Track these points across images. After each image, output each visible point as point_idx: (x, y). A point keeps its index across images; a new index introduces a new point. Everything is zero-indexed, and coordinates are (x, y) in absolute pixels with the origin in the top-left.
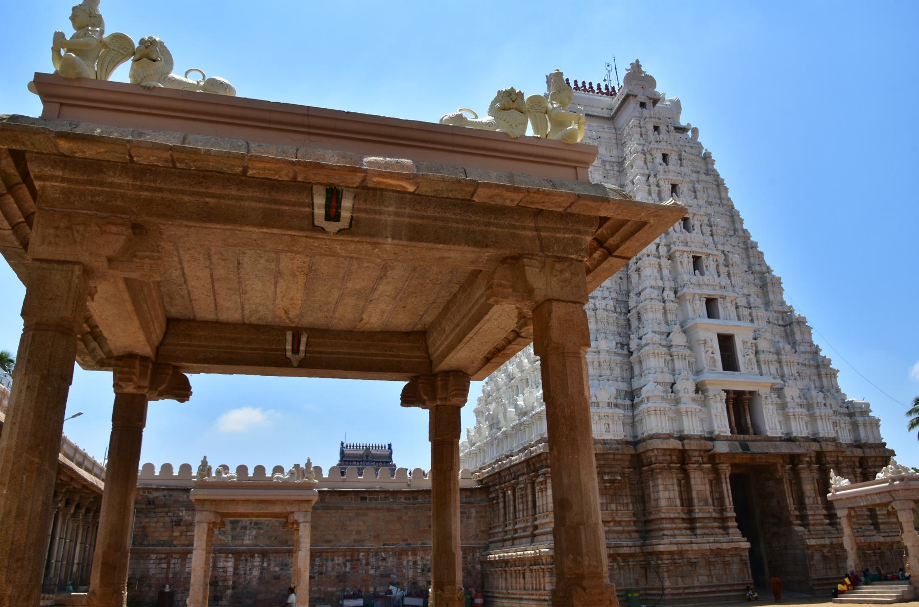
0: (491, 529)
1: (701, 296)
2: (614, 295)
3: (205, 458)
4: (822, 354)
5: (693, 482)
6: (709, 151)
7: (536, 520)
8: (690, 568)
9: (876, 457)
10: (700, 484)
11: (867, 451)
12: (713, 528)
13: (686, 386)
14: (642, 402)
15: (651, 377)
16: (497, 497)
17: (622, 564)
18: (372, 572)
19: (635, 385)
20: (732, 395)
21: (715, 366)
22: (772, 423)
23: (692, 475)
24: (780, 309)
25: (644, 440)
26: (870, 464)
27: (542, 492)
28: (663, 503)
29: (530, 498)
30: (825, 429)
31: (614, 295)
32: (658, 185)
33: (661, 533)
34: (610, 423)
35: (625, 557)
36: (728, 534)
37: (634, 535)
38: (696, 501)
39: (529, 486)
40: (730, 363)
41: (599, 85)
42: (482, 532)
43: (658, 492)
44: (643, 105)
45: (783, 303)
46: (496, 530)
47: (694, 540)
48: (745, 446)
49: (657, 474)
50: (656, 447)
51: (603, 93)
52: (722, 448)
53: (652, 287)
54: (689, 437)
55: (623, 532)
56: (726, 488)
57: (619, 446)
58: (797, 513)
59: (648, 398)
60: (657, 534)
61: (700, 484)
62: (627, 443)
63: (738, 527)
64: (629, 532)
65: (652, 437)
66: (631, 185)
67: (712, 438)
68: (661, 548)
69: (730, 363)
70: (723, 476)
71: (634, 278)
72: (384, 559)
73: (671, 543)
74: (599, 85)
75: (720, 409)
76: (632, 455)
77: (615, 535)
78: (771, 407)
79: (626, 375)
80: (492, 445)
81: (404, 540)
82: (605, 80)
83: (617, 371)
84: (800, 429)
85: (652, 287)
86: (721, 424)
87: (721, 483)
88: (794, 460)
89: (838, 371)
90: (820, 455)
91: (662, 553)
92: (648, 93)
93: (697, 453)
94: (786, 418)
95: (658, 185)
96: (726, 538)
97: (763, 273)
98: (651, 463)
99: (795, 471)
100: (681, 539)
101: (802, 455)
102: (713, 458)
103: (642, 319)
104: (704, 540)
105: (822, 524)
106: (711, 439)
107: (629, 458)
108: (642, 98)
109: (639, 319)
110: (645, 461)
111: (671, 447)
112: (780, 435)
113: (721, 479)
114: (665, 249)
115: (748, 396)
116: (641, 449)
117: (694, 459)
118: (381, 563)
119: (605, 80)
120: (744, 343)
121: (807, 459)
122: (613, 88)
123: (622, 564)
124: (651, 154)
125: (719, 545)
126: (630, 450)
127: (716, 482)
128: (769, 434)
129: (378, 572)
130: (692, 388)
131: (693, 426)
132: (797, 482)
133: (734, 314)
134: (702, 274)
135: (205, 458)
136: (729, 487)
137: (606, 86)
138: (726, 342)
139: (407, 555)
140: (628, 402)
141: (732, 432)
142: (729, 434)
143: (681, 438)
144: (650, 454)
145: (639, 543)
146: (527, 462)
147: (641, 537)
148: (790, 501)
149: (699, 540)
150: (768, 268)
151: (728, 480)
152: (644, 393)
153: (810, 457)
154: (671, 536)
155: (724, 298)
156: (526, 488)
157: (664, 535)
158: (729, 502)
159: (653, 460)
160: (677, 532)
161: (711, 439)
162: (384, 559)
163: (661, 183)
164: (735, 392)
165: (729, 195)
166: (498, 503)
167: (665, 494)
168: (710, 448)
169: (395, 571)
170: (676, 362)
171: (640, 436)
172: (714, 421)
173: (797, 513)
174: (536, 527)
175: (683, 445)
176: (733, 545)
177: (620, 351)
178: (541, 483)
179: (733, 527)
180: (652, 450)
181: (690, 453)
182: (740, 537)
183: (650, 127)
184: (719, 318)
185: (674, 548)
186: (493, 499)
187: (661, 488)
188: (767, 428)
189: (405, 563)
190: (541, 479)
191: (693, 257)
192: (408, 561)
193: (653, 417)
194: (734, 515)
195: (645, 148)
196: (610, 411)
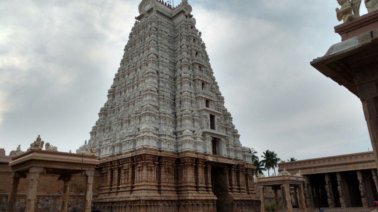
0: (100, 187)
1: (205, 98)
2: (170, 92)
3: (39, 136)
4: (235, 128)
5: (199, 172)
7: (119, 185)
8: (197, 207)
9: (250, 169)
10: (201, 172)
11: (248, 166)
12: (204, 191)
13: (199, 133)
14: (183, 137)
15: (188, 127)
16: (107, 173)
17: (170, 204)
18: (40, 207)
19: (179, 129)
21: (208, 127)
22: (224, 152)
23: (199, 169)
25: (182, 153)
26: (249, 171)
27: (139, 171)
28: (189, 180)
29: (130, 174)
30: (240, 156)
31: (170, 92)
33: (187, 192)
34: (170, 144)
35: (172, 201)
36: (209, 194)
37: (175, 192)
38: (199, 179)
39: (130, 169)
40: (213, 127)
41: (166, 3)
42: (96, 188)
43: (187, 174)
44: (186, 16)
45: (224, 107)
46: (105, 188)
47: (198, 195)
48: (217, 160)
49: (188, 167)
50: (189, 156)
51: (166, 6)
52: (210, 159)
53: (187, 91)
54: (199, 153)
55: (170, 190)
56: (209, 175)
57: (173, 154)
58: (230, 187)
59: (186, 136)
60: (184, 192)
61: (201, 172)
62: (174, 153)
63: (212, 191)
64: (173, 191)
65: (187, 152)
66: (180, 48)
67: (205, 154)
68: (189, 198)
69: (213, 127)
70: (209, 170)
71: (179, 87)
72: (47, 201)
73: (192, 196)
74: (166, 3)
76: (177, 159)
77: (168, 192)
78: (225, 145)
79: (174, 125)
80: (107, 149)
81: (58, 191)
82: (168, 2)
83: (171, 123)
84: (232, 155)
85: (187, 91)
86: (210, 150)
87: (208, 173)
88: (230, 166)
89: (240, 136)
90: (238, 165)
91: (189, 200)
92: (189, 13)
93: (202, 160)
94: (228, 150)
95: (191, 51)
96: (209, 195)
97: (218, 94)
98: (185, 162)
99: (230, 171)
100: (194, 195)
101: (233, 165)
102: (207, 163)
103: (183, 104)
104: (203, 195)
105: (237, 192)
106: (206, 155)
107: (175, 160)
108: (187, 13)
109: (180, 103)
110: (182, 161)
112: (227, 156)
113: (208, 171)
114: (193, 77)
116: (181, 156)
117: (200, 162)
118: (45, 202)
119: (168, 2)
120: (218, 119)
121: (234, 167)
122: (171, 6)
123: (170, 204)
124: (189, 38)
125: (207, 198)
126: (176, 156)
127: (206, 173)
128: (223, 156)
129: (43, 207)
130: (201, 134)
131: (200, 149)
132: (230, 176)
133: (214, 108)
135: (39, 136)
136: (210, 175)
137: (168, 4)
138: (212, 117)
139: (59, 199)
140: (175, 136)
142: (211, 154)
143: (197, 153)
144: (186, 159)
145: (177, 195)
146: (132, 158)
147: (177, 194)
148: (228, 182)
149: (200, 195)
150: (220, 93)
151: (210, 172)
152: (185, 133)
153: (235, 166)
154: (191, 193)
155: (211, 100)
156: (128, 169)
157: (189, 193)
158: (210, 181)
159: (186, 161)
160: (193, 192)
161: (206, 155)
162: (47, 201)
163: (193, 50)
164: (214, 138)
165: (210, 62)
166: (107, 176)
167: (189, 176)
168: (206, 159)
169: (52, 206)
170: (195, 123)
171: (179, 151)
172: (207, 148)
173: (230, 187)
174: (133, 187)
175: (198, 156)
176: (212, 198)
177: (172, 115)
178: (140, 167)
179: (210, 191)
180: (187, 157)
181: (200, 160)
182: (213, 195)
183: (190, 26)
184: (209, 108)
185: (193, 198)
186: (104, 173)
187: (188, 173)
189: (58, 203)
190: (139, 165)
191: (202, 83)
192: (59, 202)
194: (211, 186)
195: (187, 35)
196: (169, 139)
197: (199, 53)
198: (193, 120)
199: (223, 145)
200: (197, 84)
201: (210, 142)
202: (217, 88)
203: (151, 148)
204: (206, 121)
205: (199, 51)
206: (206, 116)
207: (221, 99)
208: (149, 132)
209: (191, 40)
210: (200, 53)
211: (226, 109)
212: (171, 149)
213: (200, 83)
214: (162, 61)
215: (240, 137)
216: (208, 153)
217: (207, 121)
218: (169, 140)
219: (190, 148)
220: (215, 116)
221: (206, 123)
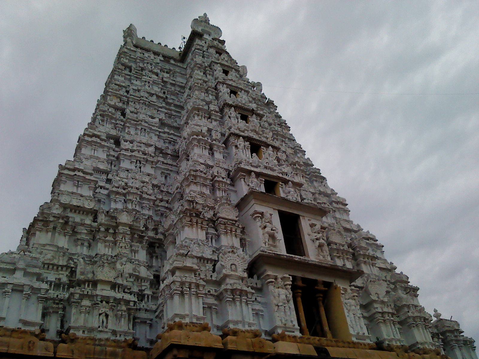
6: (271, 99)
20: (300, 283)
24: (348, 226)
32: (216, 88)
57: (119, 350)
75: (283, 297)
94: (371, 320)
111: (203, 344)
115: (321, 287)
120: (312, 226)
128: (354, 339)
134: (260, 157)
141: (301, 331)
142: (298, 334)
164: (304, 280)
188: (352, 331)
193: (176, 298)
197: (239, 93)
198: (216, 231)
199: (347, 301)
200: (234, 147)
201: (283, 292)
202: (322, 182)
203: (7, 330)
204: (265, 227)
205: (237, 87)
206: (262, 214)
207: (337, 203)
208: (13, 271)
209: (217, 71)
210: (243, 91)
211: (358, 226)
212: (114, 333)
213: (243, 144)
214: (136, 119)
215: (418, 293)
216: (280, 331)
217: (268, 229)
218: (106, 300)
219: (187, 312)
220: (301, 218)
221: (267, 235)
